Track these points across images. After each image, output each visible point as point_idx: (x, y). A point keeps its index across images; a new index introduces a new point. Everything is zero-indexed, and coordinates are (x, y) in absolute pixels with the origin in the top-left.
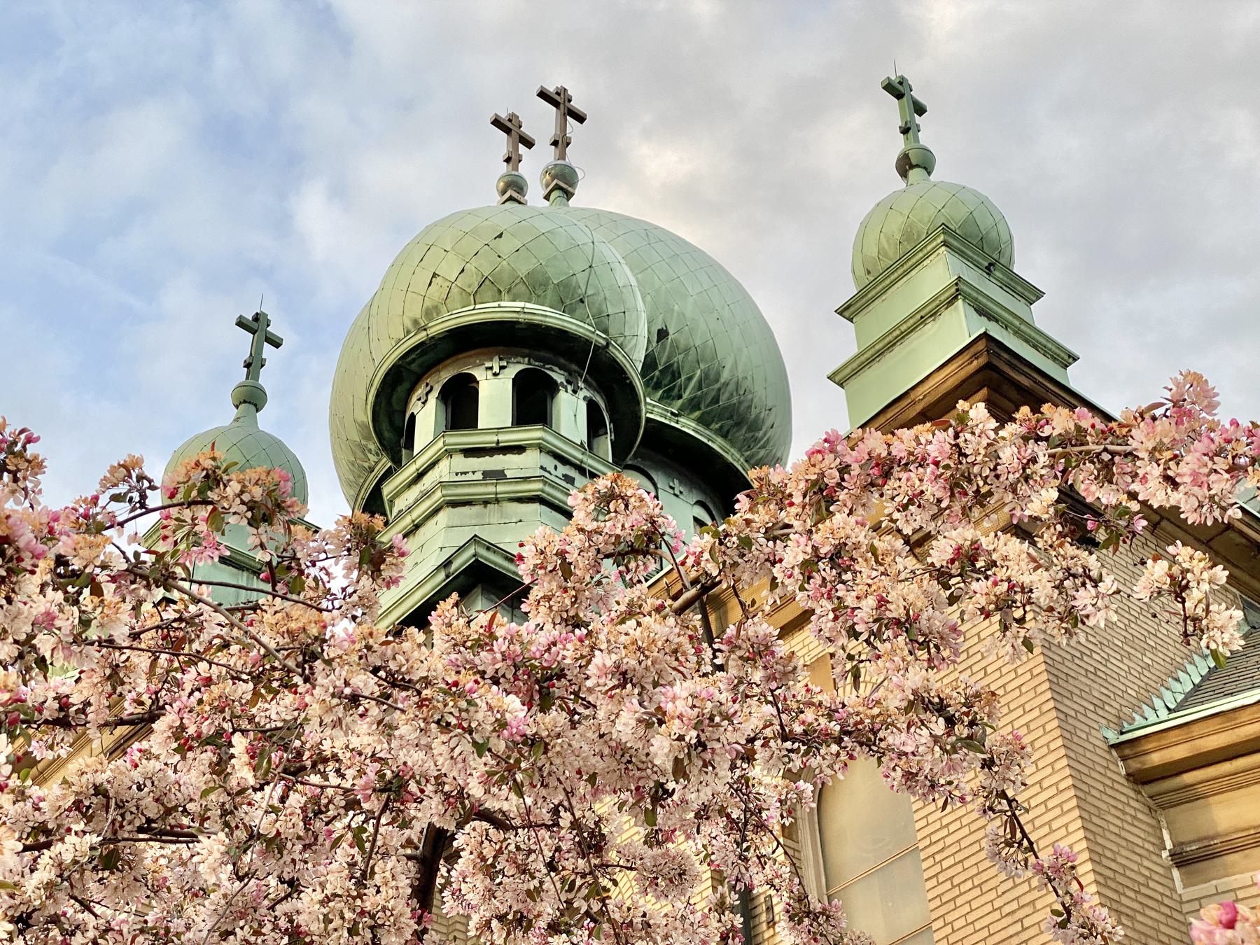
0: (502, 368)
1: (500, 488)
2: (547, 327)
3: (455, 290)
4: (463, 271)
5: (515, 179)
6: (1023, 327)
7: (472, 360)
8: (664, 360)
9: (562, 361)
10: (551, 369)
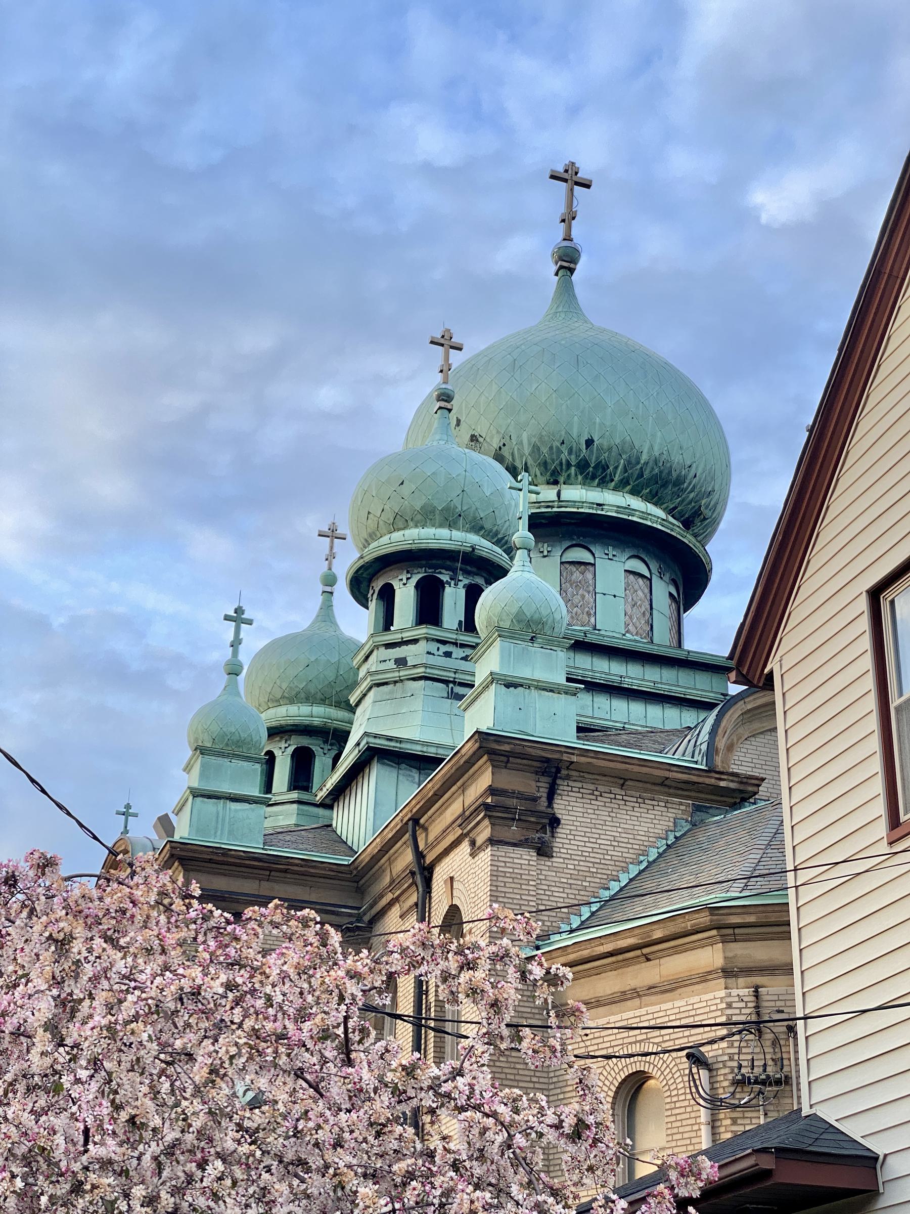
0: (408, 579)
1: (402, 673)
2: (430, 549)
3: (381, 523)
4: (383, 510)
5: (442, 391)
6: (539, 684)
7: (392, 573)
8: (593, 461)
9: (448, 563)
10: (440, 573)
